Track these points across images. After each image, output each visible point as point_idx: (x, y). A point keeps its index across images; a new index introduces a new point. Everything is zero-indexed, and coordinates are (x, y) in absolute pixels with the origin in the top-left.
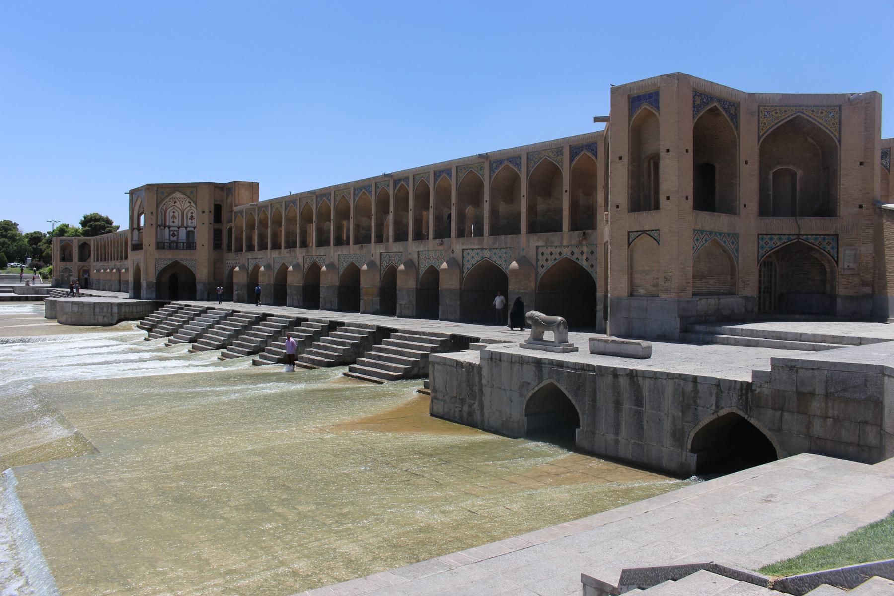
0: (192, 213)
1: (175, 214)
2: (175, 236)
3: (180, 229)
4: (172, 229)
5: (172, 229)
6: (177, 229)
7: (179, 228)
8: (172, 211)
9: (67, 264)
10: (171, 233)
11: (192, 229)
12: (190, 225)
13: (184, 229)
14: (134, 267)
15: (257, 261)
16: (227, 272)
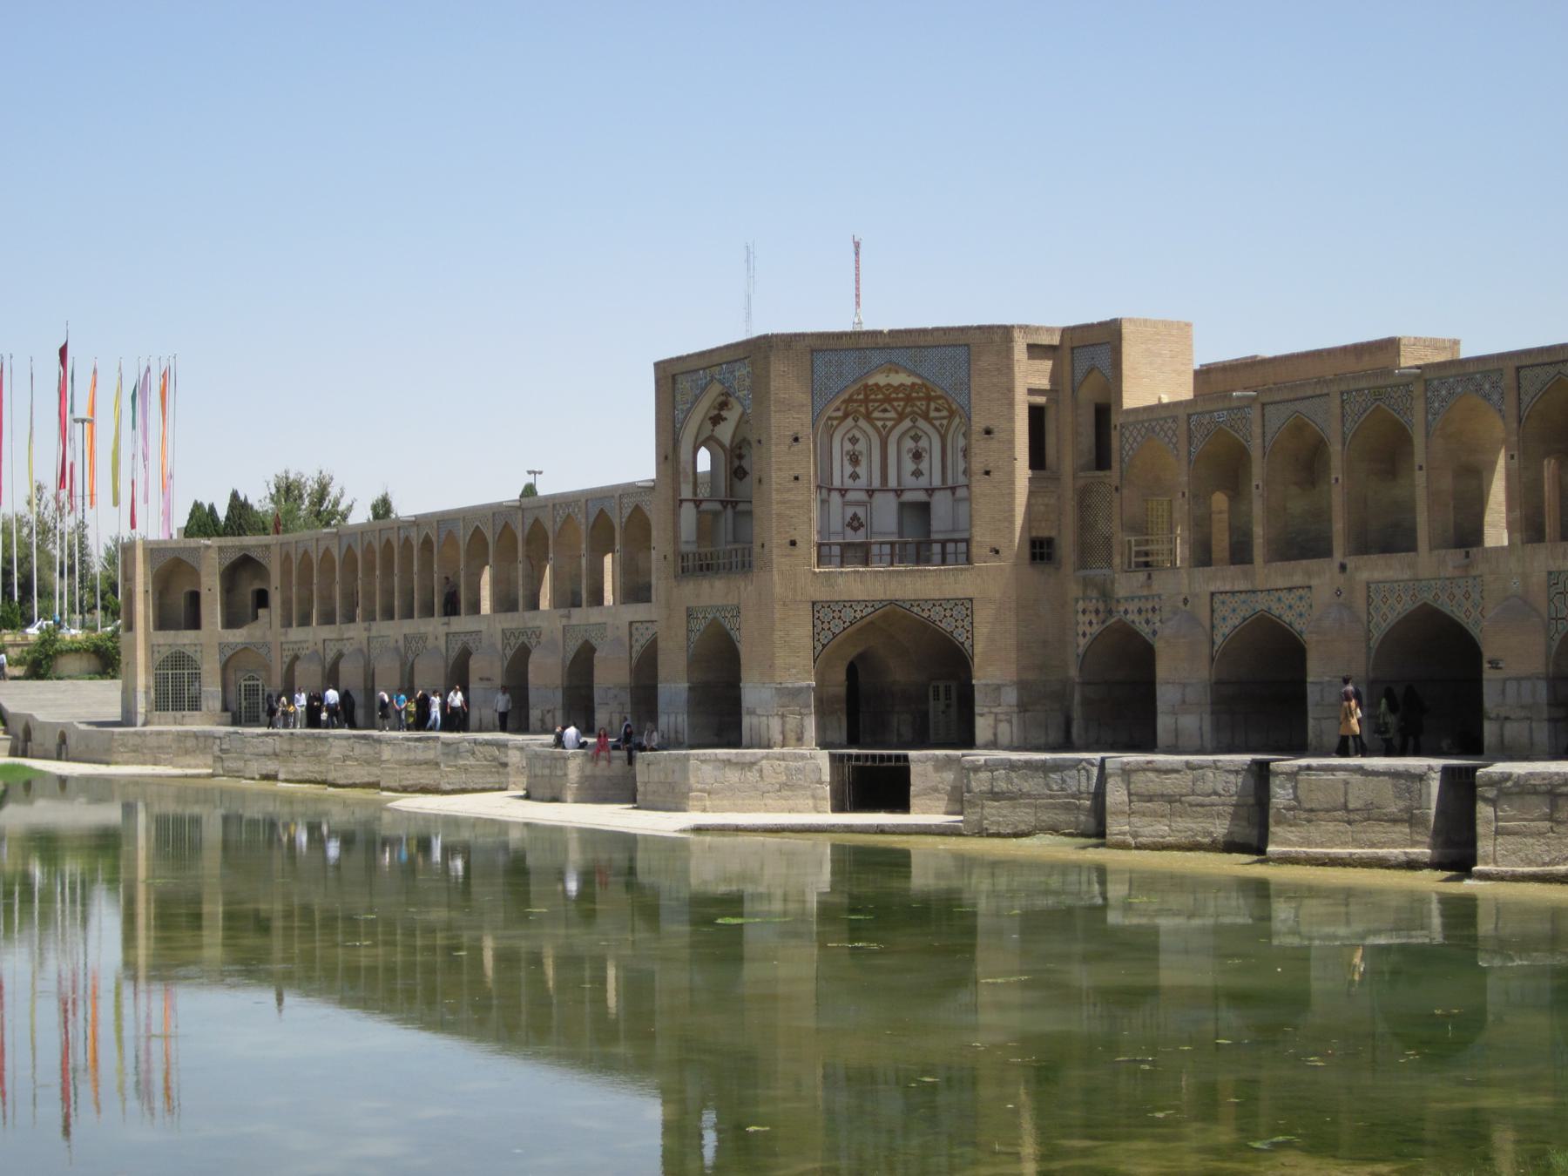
0: (916, 438)
1: (858, 447)
2: (861, 525)
3: (877, 495)
4: (851, 496)
5: (851, 496)
6: (863, 496)
7: (871, 492)
8: (850, 435)
9: (186, 638)
10: (850, 511)
11: (921, 497)
12: (909, 481)
13: (891, 496)
14: (695, 637)
15: (1261, 603)
16: (1082, 642)
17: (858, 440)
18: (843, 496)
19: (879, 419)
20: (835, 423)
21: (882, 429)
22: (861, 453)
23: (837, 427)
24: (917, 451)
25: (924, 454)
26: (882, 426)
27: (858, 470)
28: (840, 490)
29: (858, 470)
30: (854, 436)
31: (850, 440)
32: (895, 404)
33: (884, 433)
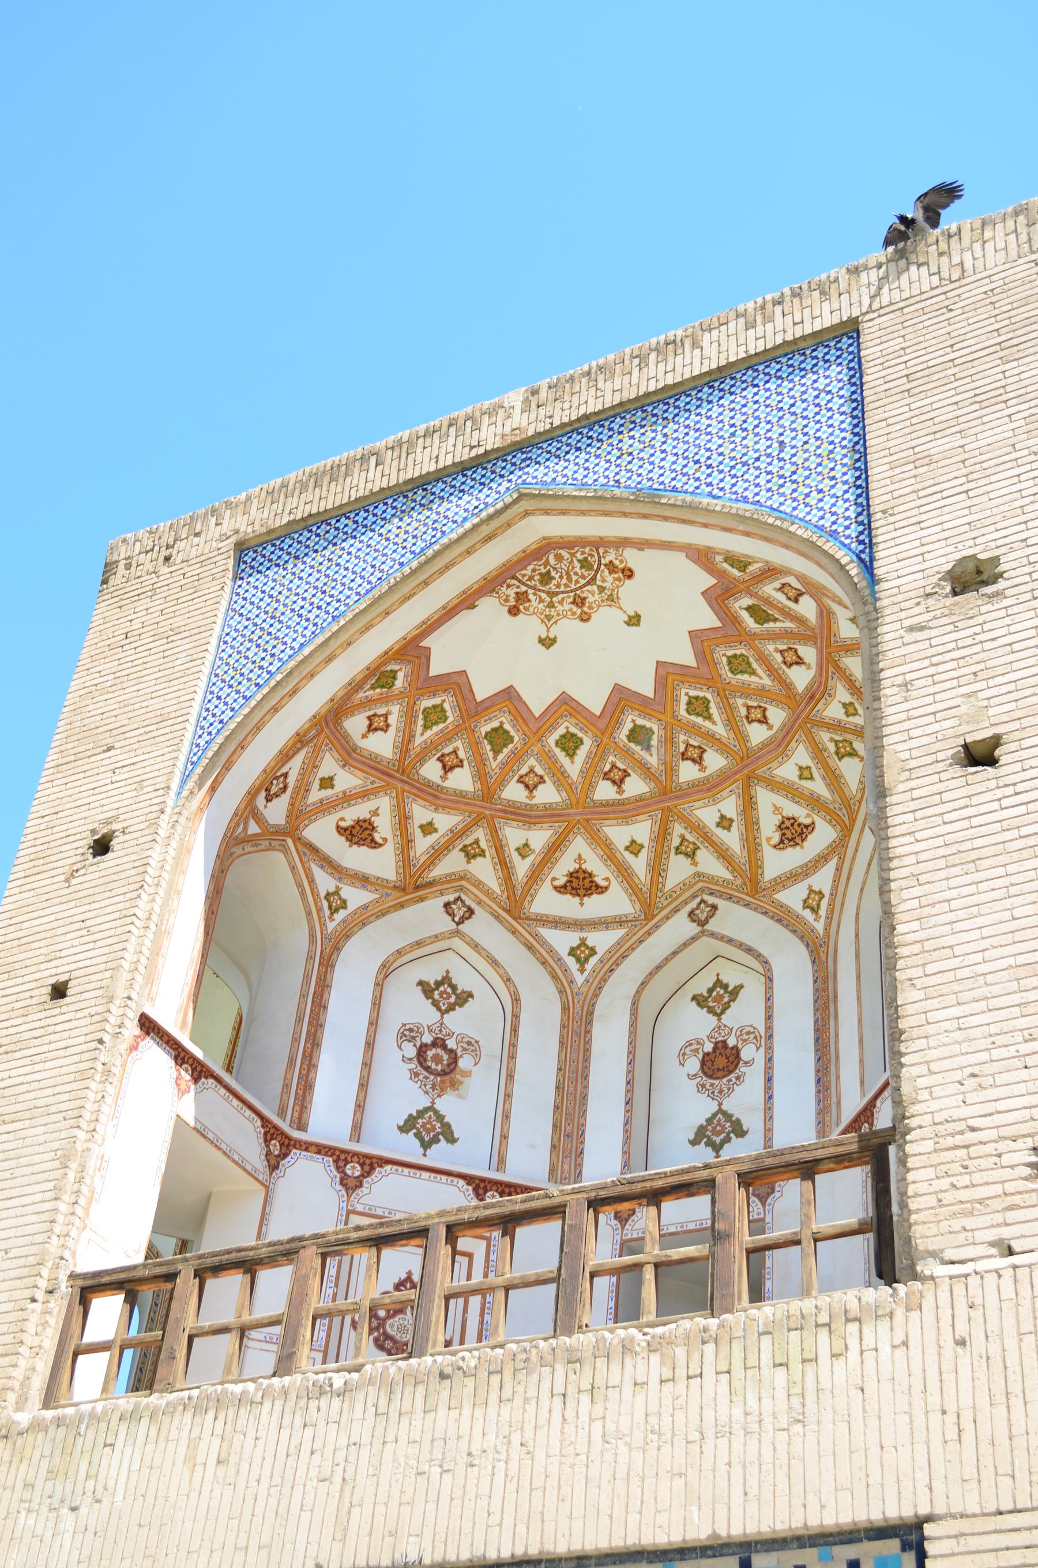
1: (458, 1022)
17: (464, 998)
18: (350, 1185)
19: (559, 923)
20: (356, 897)
21: (571, 963)
22: (472, 1046)
23: (363, 918)
24: (721, 1046)
25: (746, 1054)
26: (572, 952)
27: (447, 1105)
28: (339, 1157)
29: (447, 1105)
30: (446, 980)
31: (426, 988)
32: (619, 834)
33: (580, 979)
